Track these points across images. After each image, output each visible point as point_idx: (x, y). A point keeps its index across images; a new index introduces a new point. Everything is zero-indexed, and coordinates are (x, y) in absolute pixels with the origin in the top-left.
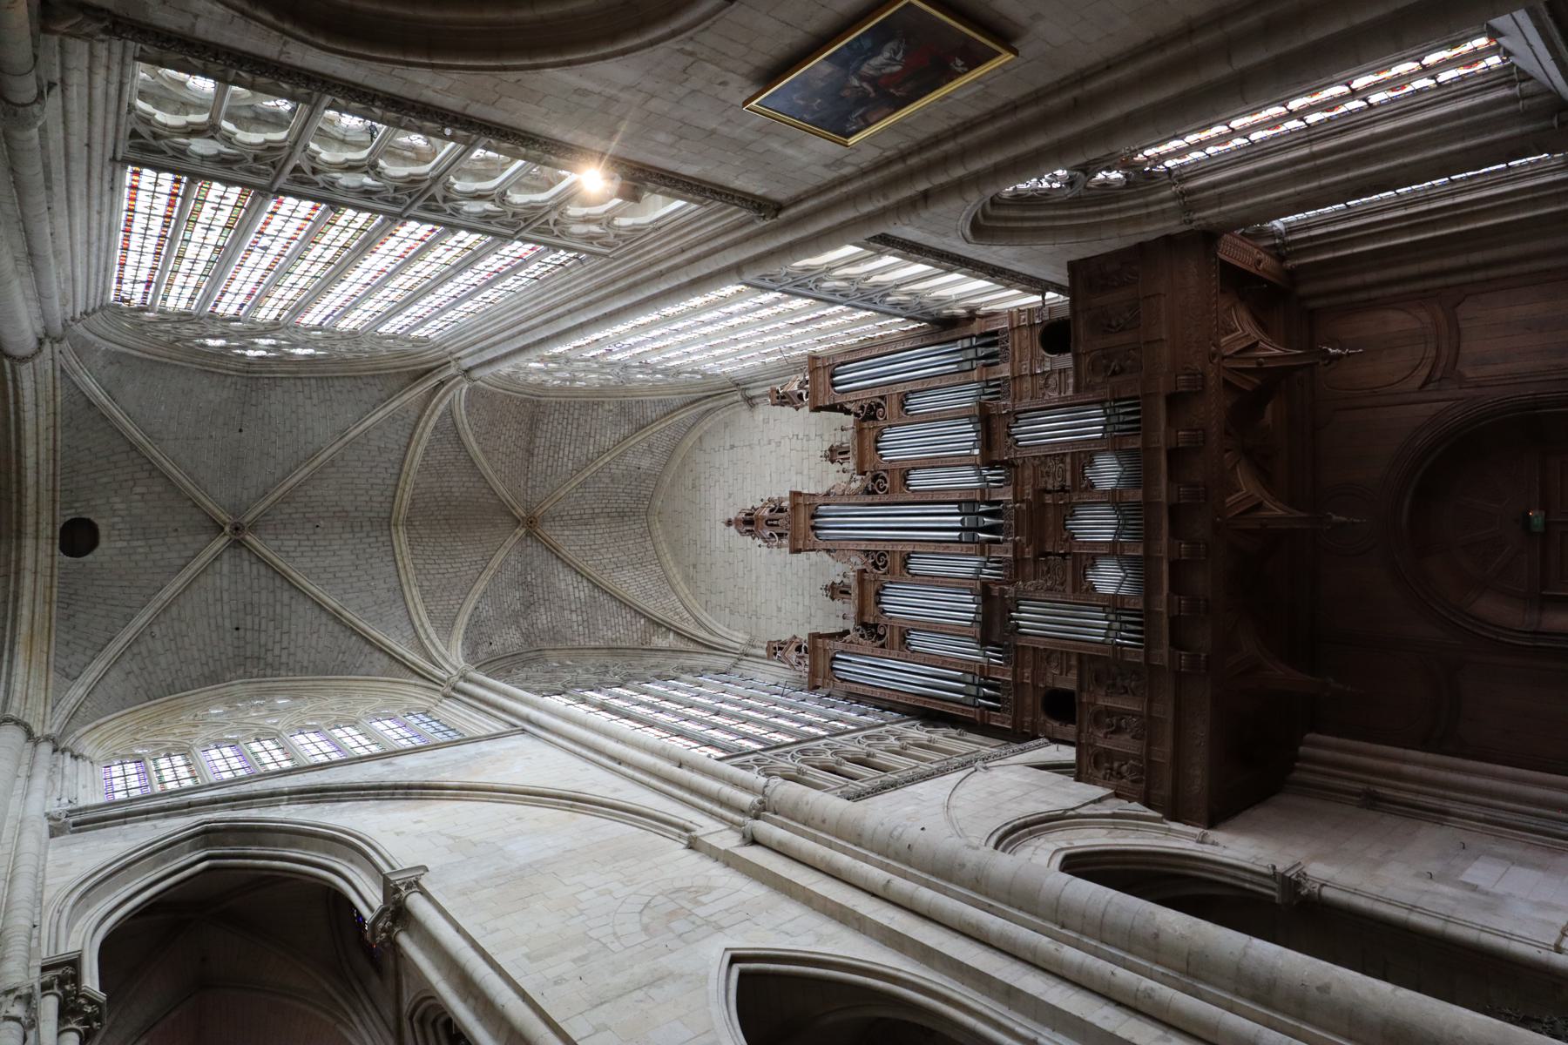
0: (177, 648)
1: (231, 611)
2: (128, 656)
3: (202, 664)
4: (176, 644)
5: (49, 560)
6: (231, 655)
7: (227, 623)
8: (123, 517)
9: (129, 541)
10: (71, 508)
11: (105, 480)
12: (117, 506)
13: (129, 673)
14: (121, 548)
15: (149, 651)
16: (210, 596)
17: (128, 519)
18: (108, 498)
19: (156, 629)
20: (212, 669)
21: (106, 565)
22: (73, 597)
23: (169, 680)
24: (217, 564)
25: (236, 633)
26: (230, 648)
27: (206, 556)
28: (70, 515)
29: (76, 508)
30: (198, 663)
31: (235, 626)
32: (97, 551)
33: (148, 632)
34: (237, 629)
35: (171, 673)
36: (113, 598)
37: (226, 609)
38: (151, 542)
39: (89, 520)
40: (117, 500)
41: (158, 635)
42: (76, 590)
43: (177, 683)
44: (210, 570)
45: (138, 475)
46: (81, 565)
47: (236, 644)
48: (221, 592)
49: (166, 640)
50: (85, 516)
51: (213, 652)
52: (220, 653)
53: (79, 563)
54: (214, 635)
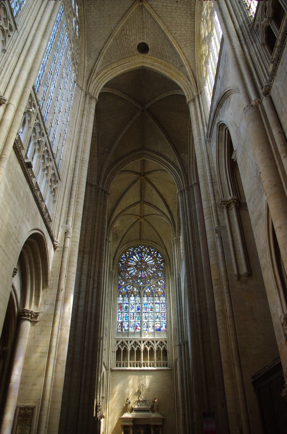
0: (180, 26)
1: (171, 3)
2: (180, 44)
3: (187, 18)
4: (179, 26)
5: (149, 59)
6: (186, 6)
7: (175, 5)
8: (137, 36)
9: (144, 34)
10: (134, 52)
11: (125, 44)
12: (133, 38)
13: (185, 45)
14: (147, 37)
15: (180, 36)
16: (164, 10)
17: (137, 34)
18: (131, 42)
19: (173, 32)
20: (189, 15)
21: (152, 42)
22: (160, 54)
23: (190, 32)
24: (153, 6)
25: (179, 3)
26: (184, 6)
27: (151, 11)
28: (136, 52)
29: (134, 51)
30: (187, 20)
31: (176, 2)
32: (148, 44)
33: (173, 35)
34: (177, 2)
35: (188, 31)
36: (162, 42)
37: (169, 5)
38: (145, 27)
39: (138, 46)
40: (131, 38)
41: (175, 31)
42: (158, 52)
43: (192, 30)
44: (155, 9)
45: (123, 34)
46: (151, 49)
47: (183, 4)
48: (163, 6)
49: (177, 29)
50: (137, 47)
51: (184, 13)
52: (185, 10)
53: (150, 50)
54: (178, 11)
